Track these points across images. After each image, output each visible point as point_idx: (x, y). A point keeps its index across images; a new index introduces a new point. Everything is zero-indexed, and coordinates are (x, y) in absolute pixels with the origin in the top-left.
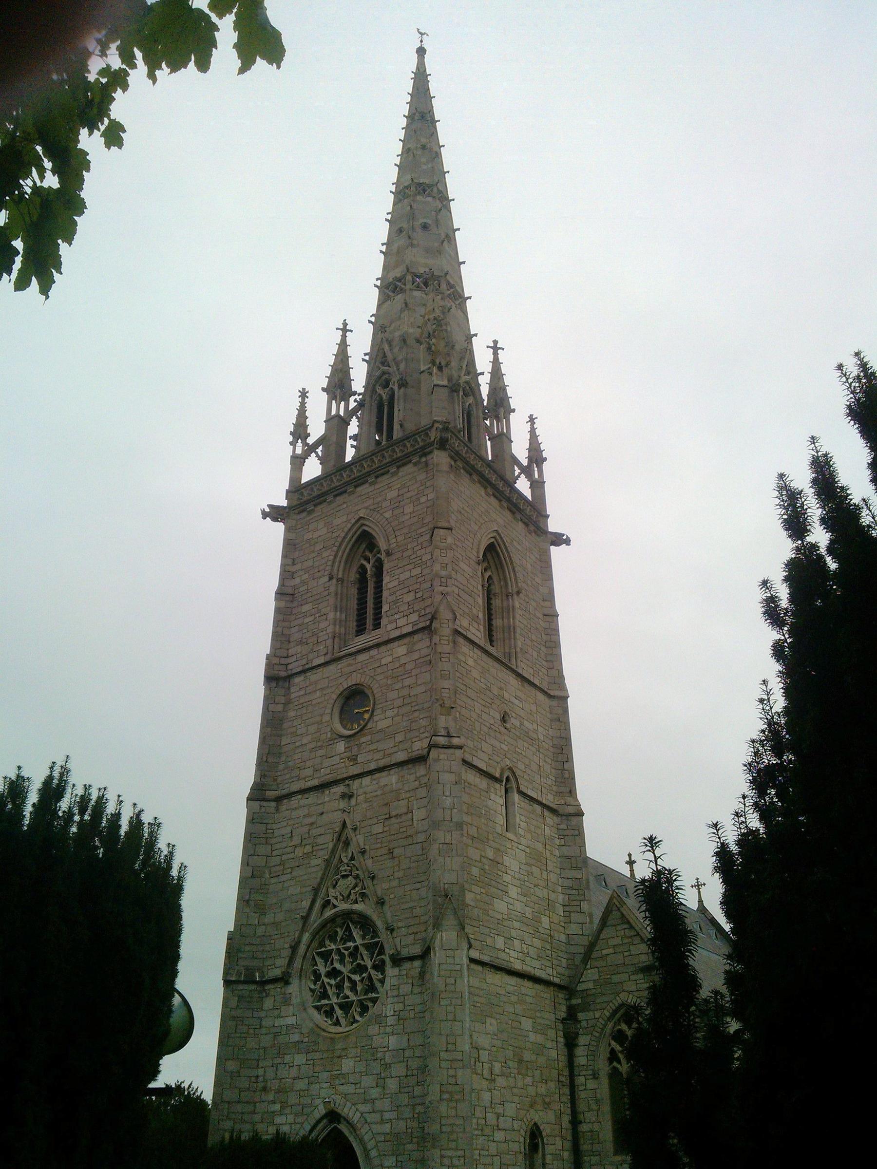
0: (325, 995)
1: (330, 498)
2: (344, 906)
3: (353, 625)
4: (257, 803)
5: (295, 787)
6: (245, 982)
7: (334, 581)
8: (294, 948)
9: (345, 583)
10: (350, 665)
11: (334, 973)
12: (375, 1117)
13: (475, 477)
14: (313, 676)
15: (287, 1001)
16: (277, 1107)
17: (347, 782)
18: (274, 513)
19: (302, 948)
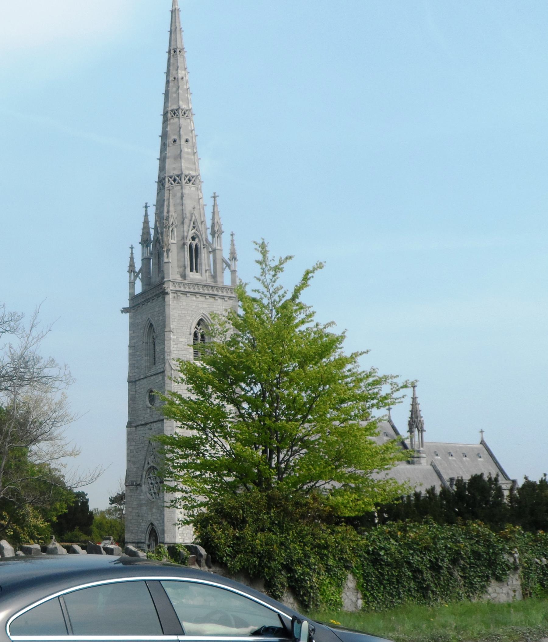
0: (150, 490)
1: (141, 306)
2: (152, 464)
3: (152, 360)
4: (129, 428)
5: (140, 423)
6: (131, 485)
7: (144, 344)
8: (142, 476)
9: (148, 344)
10: (149, 380)
11: (152, 484)
12: (159, 525)
13: (188, 295)
14: (142, 382)
15: (142, 491)
16: (141, 521)
17: (150, 424)
18: (125, 310)
19: (144, 476)
